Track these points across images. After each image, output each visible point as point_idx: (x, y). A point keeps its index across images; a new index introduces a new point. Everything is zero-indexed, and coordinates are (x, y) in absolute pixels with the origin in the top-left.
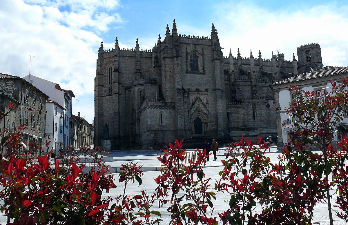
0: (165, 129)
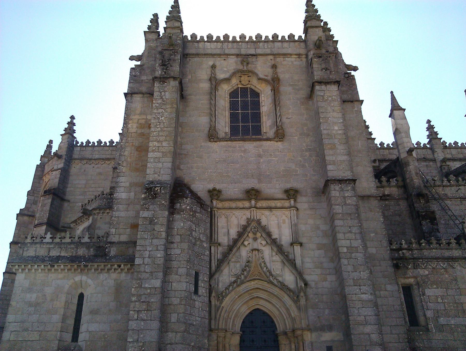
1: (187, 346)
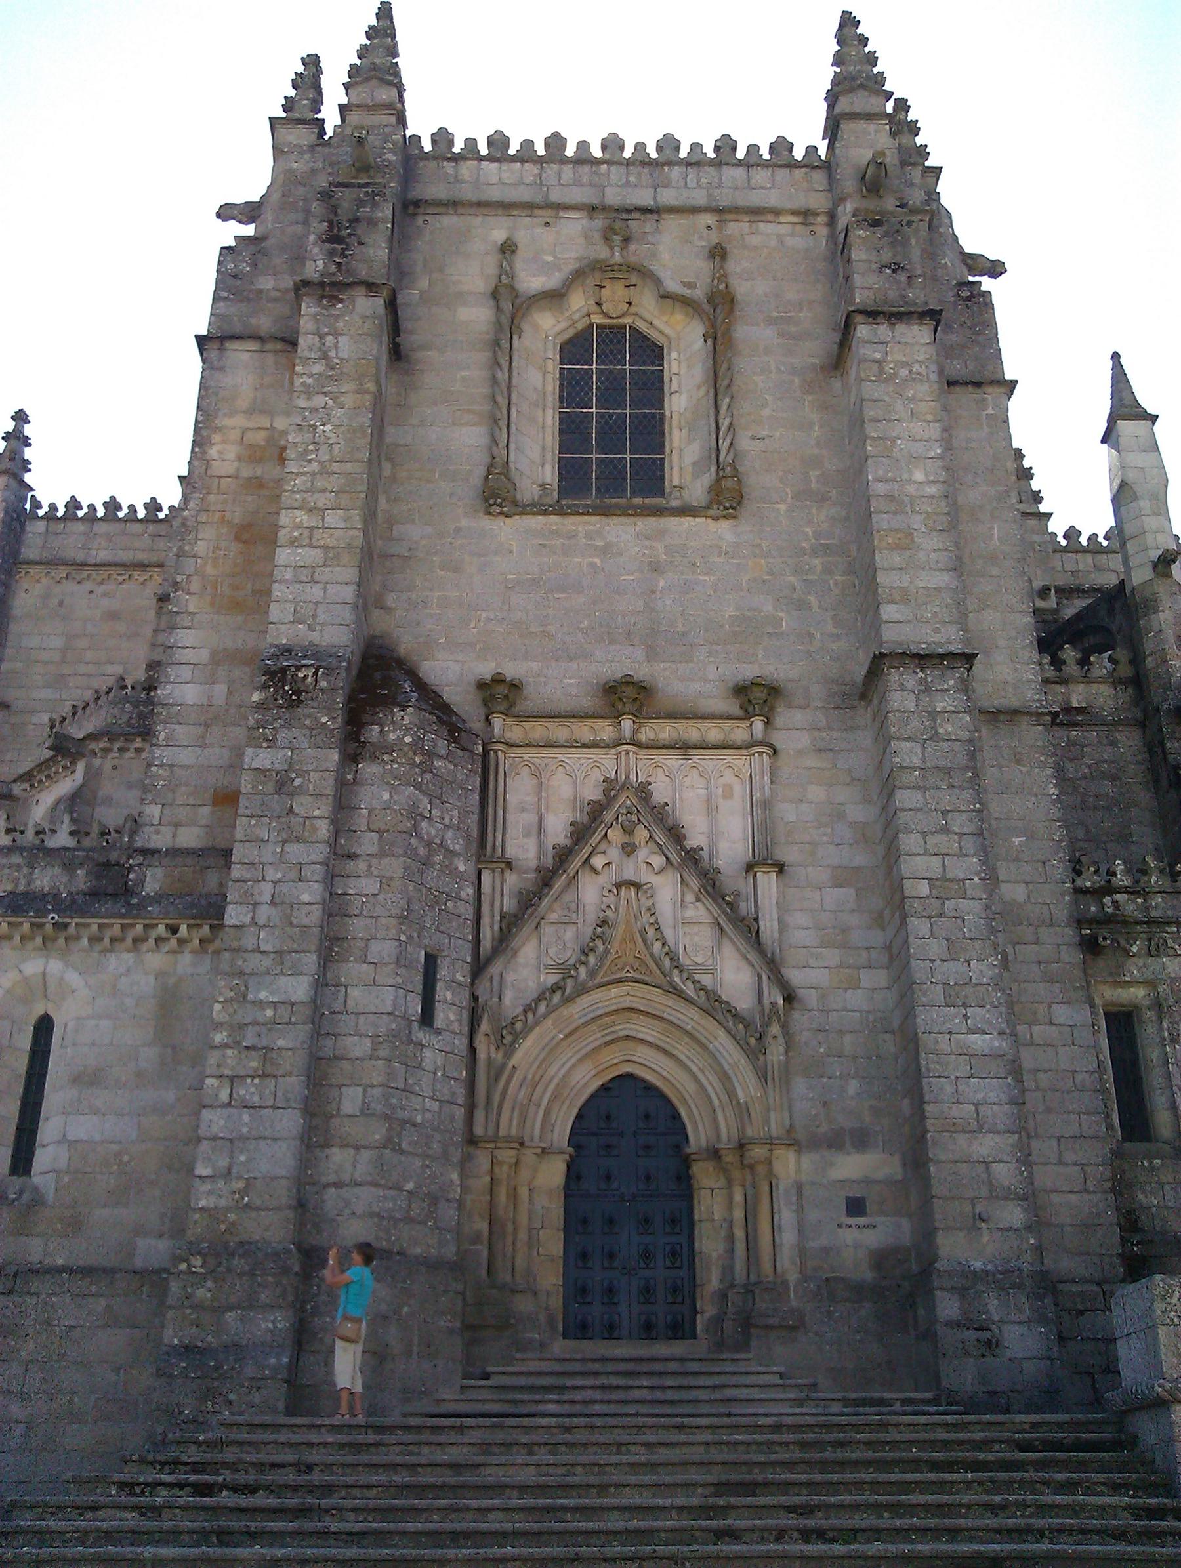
0: (35, 1250)
1: (393, 1192)
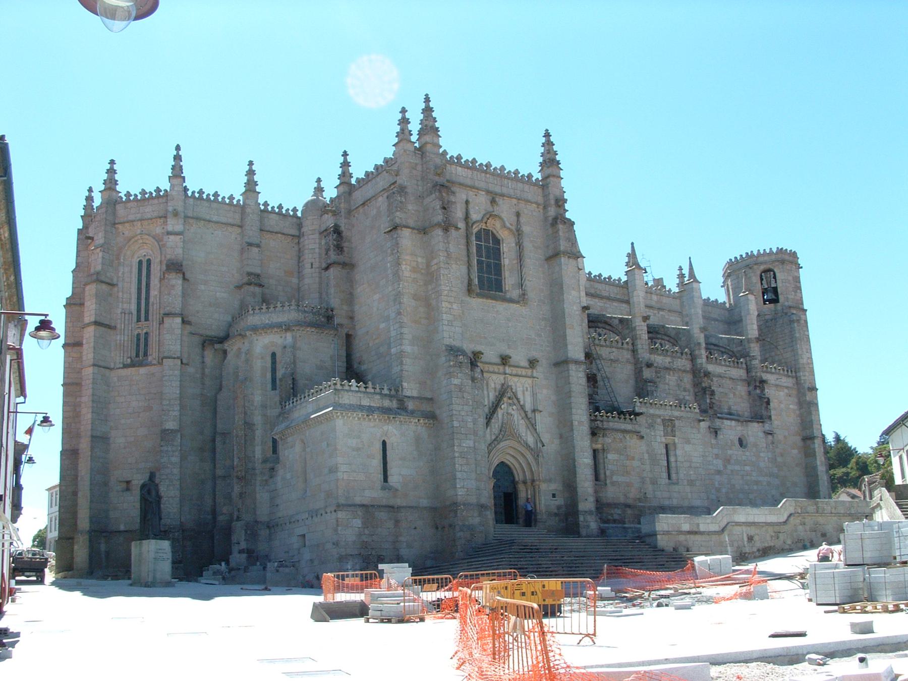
0: (399, 502)
